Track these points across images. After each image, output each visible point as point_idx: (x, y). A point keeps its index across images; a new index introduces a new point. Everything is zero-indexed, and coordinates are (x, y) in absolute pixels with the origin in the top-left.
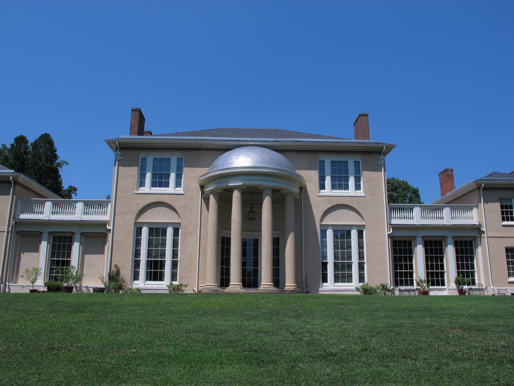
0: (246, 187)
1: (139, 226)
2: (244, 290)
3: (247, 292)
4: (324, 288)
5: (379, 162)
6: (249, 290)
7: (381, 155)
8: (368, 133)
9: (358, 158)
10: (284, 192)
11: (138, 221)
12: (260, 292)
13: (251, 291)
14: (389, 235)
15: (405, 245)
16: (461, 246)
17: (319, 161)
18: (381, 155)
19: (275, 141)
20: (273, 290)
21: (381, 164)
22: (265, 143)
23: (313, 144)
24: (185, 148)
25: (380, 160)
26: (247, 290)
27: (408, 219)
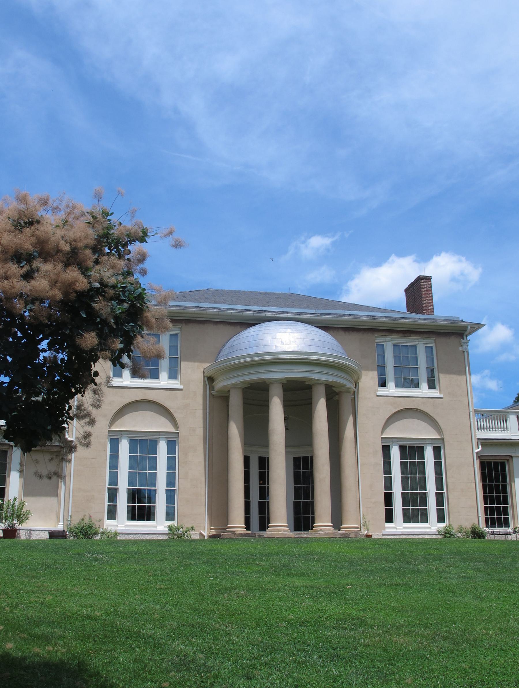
0: (287, 381)
1: (115, 436)
2: (293, 535)
3: (299, 536)
4: (387, 530)
5: (460, 349)
6: (302, 534)
7: (463, 339)
8: (431, 305)
9: (430, 342)
10: (337, 390)
11: (112, 429)
12: (317, 535)
13: (303, 534)
14: (477, 453)
15: (496, 469)
16: (490, 469)
17: (377, 344)
18: (463, 339)
19: (316, 314)
20: (333, 533)
21: (464, 352)
22: (302, 316)
23: (371, 320)
24: (183, 320)
25: (462, 346)
26: (298, 534)
27: (480, 431)
